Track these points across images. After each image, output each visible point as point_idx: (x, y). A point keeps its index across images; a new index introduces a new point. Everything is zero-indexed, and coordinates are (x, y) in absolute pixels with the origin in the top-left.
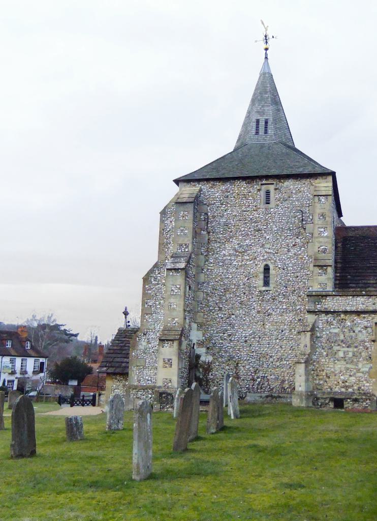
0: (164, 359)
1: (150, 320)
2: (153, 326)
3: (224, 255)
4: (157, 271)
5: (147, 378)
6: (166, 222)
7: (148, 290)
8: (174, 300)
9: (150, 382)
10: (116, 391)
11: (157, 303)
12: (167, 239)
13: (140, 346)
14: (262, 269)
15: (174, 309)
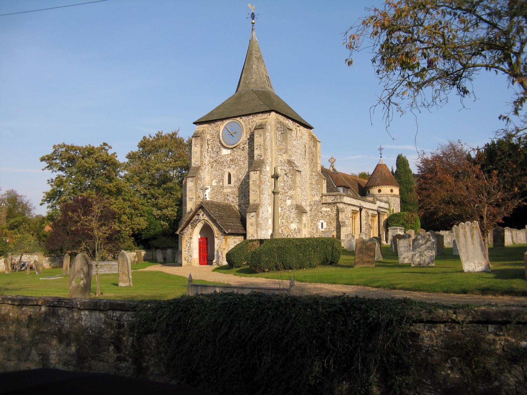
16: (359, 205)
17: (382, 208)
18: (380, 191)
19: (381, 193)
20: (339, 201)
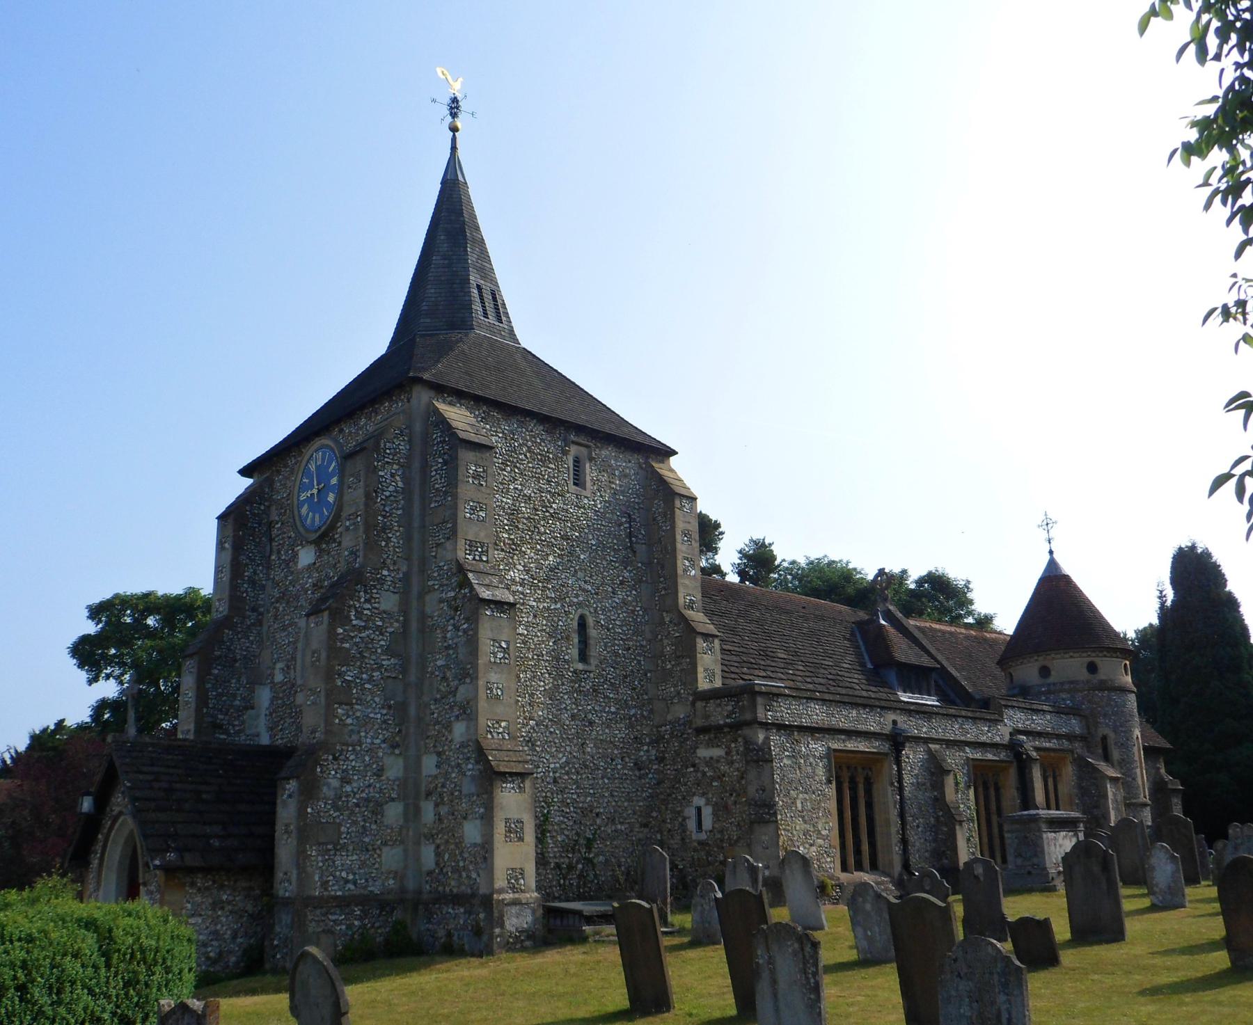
0: (507, 820)
1: (349, 721)
2: (355, 737)
3: (513, 580)
5: (344, 874)
8: (497, 676)
9: (352, 887)
11: (364, 676)
12: (384, 517)
13: (325, 789)
14: (575, 624)
15: (497, 697)
18: (1045, 672)
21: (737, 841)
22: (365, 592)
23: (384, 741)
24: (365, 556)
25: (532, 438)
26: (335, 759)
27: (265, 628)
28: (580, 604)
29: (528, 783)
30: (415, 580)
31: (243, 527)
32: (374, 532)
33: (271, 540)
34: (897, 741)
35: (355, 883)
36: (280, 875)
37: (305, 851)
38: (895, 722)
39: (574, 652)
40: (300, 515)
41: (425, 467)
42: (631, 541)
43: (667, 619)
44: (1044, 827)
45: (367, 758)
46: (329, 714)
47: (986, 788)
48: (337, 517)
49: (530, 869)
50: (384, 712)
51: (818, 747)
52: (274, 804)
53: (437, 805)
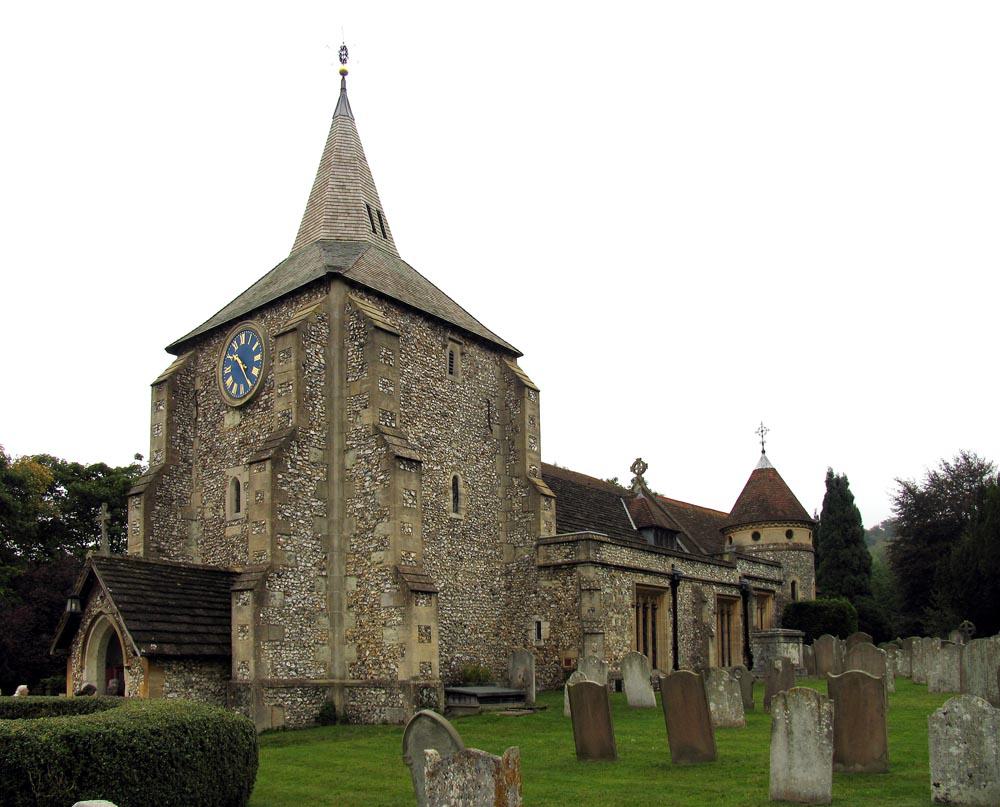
0: (419, 627)
2: (293, 561)
4: (296, 448)
5: (288, 664)
6: (308, 351)
7: (282, 484)
8: (408, 517)
9: (294, 673)
10: (170, 696)
11: (299, 514)
12: (311, 386)
15: (409, 534)
16: (668, 570)
17: (756, 579)
19: (760, 542)
20: (582, 557)
21: (569, 647)
22: (298, 446)
23: (314, 565)
24: (297, 418)
25: (419, 331)
26: (279, 576)
27: (194, 476)
28: (453, 468)
29: (433, 600)
30: (336, 440)
31: (177, 394)
32: (304, 399)
33: (197, 405)
34: (675, 580)
35: (296, 671)
36: (237, 663)
37: (259, 646)
38: (673, 566)
39: (450, 504)
40: (225, 386)
41: (343, 348)
42: (489, 421)
43: (516, 483)
44: (782, 639)
45: (302, 577)
46: (274, 543)
47: (723, 615)
48: (261, 388)
49: (436, 662)
50: (314, 542)
51: (627, 581)
52: (229, 610)
53: (358, 615)
